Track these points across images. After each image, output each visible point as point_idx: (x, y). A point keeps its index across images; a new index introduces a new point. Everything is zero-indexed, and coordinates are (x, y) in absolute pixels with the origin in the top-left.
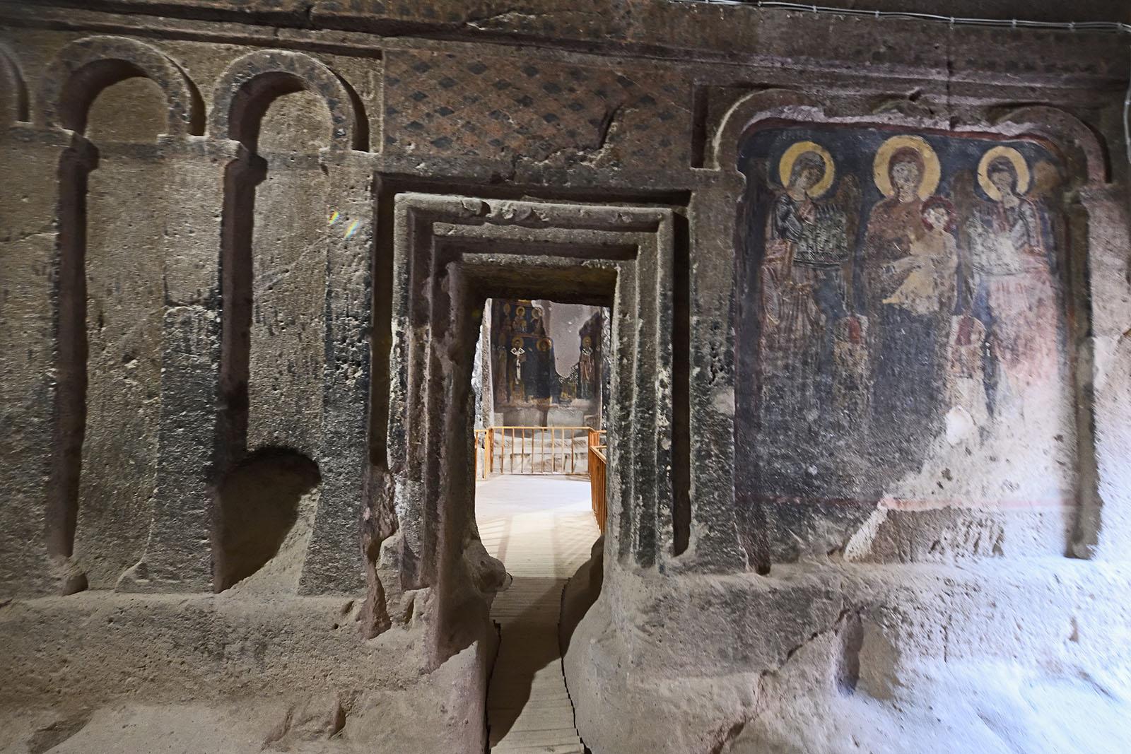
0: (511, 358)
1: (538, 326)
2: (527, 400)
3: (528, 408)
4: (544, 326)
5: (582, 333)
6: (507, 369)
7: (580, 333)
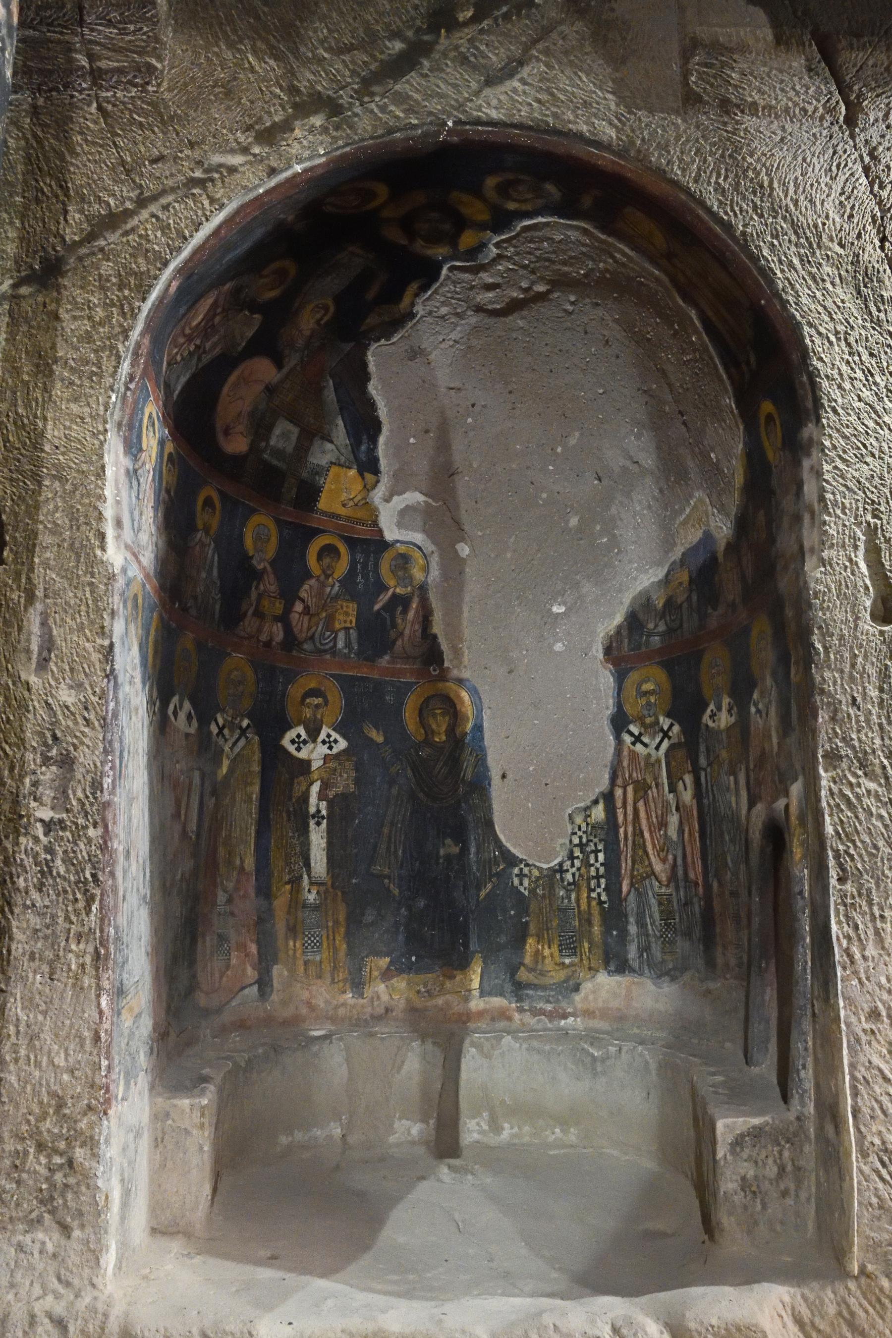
0: (281, 774)
1: (408, 623)
2: (358, 984)
3: (364, 1024)
4: (437, 628)
6: (264, 825)
7: (608, 651)
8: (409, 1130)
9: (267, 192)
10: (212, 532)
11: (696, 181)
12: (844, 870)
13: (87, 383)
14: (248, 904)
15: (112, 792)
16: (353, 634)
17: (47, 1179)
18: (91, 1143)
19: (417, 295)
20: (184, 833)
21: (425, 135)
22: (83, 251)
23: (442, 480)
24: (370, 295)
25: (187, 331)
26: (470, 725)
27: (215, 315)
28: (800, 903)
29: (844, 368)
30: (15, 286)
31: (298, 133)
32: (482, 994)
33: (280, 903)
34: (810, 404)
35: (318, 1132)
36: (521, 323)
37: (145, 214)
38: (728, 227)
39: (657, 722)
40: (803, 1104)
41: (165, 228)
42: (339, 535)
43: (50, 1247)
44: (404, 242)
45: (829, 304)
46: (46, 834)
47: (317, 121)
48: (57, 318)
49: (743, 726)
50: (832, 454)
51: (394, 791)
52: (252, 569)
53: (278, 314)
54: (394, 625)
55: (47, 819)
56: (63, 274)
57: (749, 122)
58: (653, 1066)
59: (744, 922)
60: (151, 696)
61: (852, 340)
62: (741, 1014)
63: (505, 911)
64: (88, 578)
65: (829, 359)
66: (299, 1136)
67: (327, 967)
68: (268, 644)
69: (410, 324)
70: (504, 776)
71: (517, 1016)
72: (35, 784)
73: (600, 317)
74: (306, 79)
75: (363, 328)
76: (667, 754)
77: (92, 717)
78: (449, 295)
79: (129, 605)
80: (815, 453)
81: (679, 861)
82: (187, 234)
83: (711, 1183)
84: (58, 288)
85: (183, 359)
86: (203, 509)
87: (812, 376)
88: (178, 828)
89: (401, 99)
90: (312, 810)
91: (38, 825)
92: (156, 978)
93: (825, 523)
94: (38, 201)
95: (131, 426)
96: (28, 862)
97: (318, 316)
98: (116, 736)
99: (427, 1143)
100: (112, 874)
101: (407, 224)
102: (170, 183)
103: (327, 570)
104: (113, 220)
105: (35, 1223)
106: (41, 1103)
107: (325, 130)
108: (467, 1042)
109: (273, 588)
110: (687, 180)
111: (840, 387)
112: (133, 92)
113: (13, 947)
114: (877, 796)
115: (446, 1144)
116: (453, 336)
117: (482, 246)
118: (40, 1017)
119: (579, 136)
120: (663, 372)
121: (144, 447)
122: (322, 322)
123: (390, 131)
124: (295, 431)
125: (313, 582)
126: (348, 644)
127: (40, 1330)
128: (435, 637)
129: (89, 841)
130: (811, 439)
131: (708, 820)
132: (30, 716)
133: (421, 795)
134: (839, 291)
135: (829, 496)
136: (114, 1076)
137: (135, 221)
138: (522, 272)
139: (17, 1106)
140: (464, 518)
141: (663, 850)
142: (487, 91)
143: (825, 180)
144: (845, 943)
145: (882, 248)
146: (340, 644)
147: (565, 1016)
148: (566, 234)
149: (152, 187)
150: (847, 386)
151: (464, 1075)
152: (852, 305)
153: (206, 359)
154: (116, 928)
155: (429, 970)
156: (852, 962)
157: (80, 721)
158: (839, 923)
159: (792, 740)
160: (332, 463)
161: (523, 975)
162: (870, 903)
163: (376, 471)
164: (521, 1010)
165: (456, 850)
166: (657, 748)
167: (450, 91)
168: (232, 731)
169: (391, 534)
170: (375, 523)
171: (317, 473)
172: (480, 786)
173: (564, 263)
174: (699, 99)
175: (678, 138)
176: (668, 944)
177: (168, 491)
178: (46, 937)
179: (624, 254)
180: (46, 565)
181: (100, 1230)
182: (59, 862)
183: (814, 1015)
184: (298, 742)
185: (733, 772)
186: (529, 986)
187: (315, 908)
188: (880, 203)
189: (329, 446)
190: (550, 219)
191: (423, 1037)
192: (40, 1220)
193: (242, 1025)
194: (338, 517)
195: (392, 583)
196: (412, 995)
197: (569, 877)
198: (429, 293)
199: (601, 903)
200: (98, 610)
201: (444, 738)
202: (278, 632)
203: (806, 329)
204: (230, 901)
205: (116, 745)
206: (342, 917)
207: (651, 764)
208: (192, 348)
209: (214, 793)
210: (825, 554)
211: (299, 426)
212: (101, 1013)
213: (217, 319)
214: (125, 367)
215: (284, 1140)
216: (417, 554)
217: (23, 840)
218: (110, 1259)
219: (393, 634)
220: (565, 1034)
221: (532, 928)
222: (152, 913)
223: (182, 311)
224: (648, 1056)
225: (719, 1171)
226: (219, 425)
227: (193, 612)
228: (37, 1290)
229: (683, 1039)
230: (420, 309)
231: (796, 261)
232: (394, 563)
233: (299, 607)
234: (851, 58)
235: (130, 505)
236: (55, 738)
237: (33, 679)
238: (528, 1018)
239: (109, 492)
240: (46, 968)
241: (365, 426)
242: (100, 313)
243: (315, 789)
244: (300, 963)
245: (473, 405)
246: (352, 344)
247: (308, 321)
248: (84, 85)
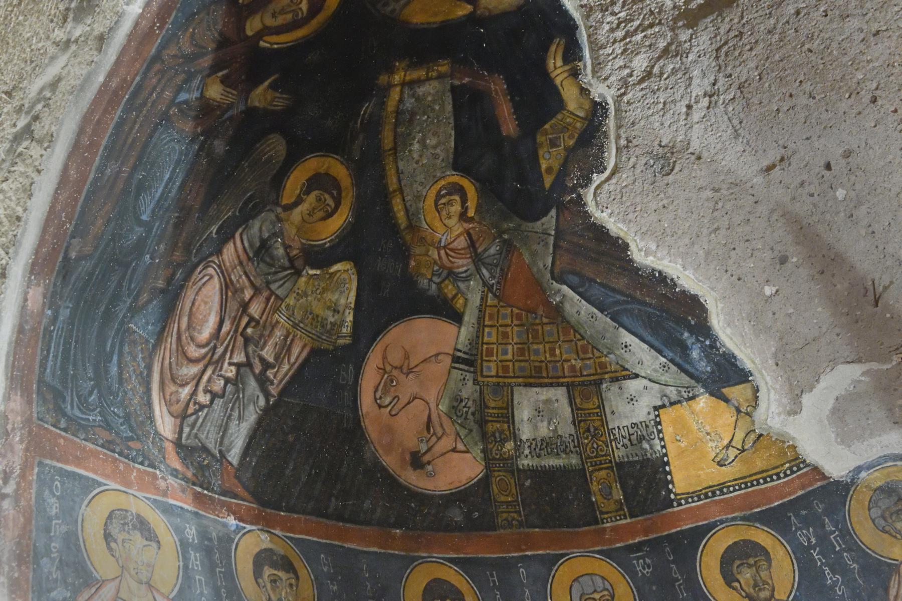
9: (110, 75)
19: (575, 74)
24: (509, 126)
27: (245, 306)
42: (743, 518)
69: (611, 122)
75: (548, 181)
78: (620, 34)
82: (19, 210)
85: (214, 396)
97: (456, 208)
122: (471, 213)
124: (559, 395)
160: (656, 408)
163: (743, 376)
169: (837, 465)
170: (798, 461)
171: (641, 439)
189: (633, 386)
194: (722, 487)
198: (587, 53)
211: (559, 385)
213: (255, 309)
223: (142, 328)
226: (390, 461)
230: (600, 91)
232: (876, 512)
241: (673, 318)
245: (828, 167)
246: (553, 212)
247: (445, 223)
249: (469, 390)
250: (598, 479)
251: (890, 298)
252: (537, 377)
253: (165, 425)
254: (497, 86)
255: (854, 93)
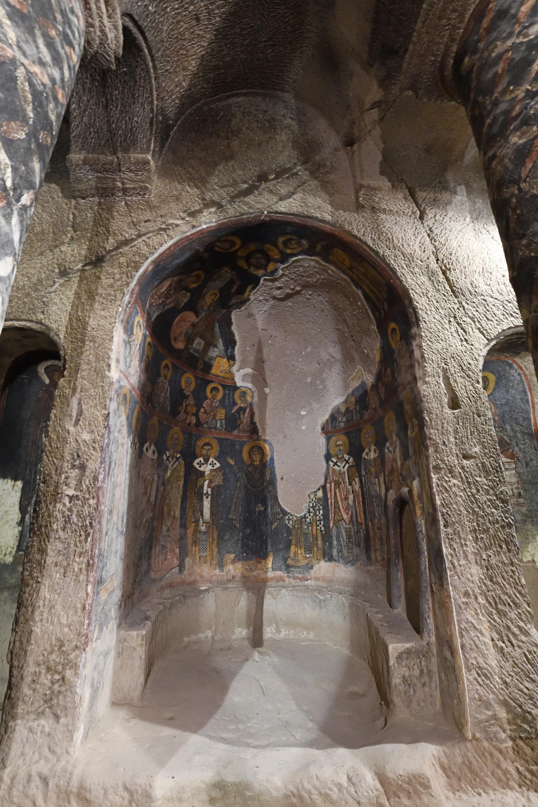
0: (192, 476)
1: (245, 418)
2: (221, 565)
3: (223, 584)
4: (257, 420)
5: (328, 430)
6: (184, 498)
8: (242, 633)
10: (168, 377)
11: (363, 236)
12: (446, 522)
13: (109, 303)
14: (176, 532)
15: (103, 482)
16: (224, 421)
17: (50, 688)
18: (75, 667)
19: (251, 291)
20: (149, 501)
21: (255, 217)
22: (113, 253)
23: (259, 364)
24: (233, 290)
25: (158, 294)
26: (269, 458)
27: (170, 290)
28: (421, 537)
29: (427, 306)
30: (83, 266)
31: (205, 214)
32: (273, 569)
33: (190, 531)
34: (414, 320)
35: (201, 635)
36: (290, 304)
37: (140, 240)
38: (377, 253)
39: (343, 457)
40: (430, 637)
41: (148, 245)
43: (47, 729)
44: (246, 267)
45: (419, 282)
46: (70, 502)
47: (213, 210)
48: (100, 278)
49: (382, 457)
50: (426, 339)
51: (238, 485)
52: (184, 394)
53: (197, 295)
54: (240, 418)
55: (71, 495)
56: (104, 262)
57: (383, 216)
58: (347, 605)
59: (385, 541)
60: (134, 440)
61: (429, 296)
62: (385, 582)
63: (282, 534)
64: (101, 384)
65: (421, 302)
66: (193, 637)
67: (208, 558)
68: (189, 424)
69: (248, 303)
70: (282, 479)
71: (287, 580)
72: (67, 478)
73: (320, 300)
74: (209, 196)
76: (348, 470)
77: (96, 446)
79: (121, 397)
80: (417, 339)
81: (354, 514)
83: (386, 676)
84: (101, 267)
86: (164, 368)
87: (414, 309)
88: (145, 499)
89: (246, 204)
90: (205, 492)
91: (67, 498)
92: (127, 569)
93: (425, 367)
94: (97, 235)
95: (128, 322)
96: (59, 516)
97: (213, 297)
98: (107, 456)
99: (249, 639)
100: (100, 522)
101: (247, 259)
102: (152, 229)
103: (214, 397)
104: (126, 242)
105: (40, 714)
106: (51, 644)
107: (216, 213)
108: (266, 592)
109: (192, 402)
110: (360, 235)
111: (426, 313)
112: (140, 197)
113: (47, 559)
114: (459, 487)
115: (257, 640)
116: (264, 309)
117: (276, 270)
118: (56, 596)
119: (317, 219)
120: (345, 320)
121: (135, 332)
123: (242, 214)
124: (203, 342)
125: (208, 401)
126: (221, 426)
127: (32, 785)
128: (255, 423)
129: (90, 506)
130: (415, 334)
131: (366, 497)
132: (68, 445)
133: (249, 486)
134: (422, 278)
135: (426, 355)
136: (91, 628)
137: (136, 243)
138: (292, 281)
139: (38, 647)
140: (267, 378)
141: (347, 509)
142: (280, 202)
143: (413, 238)
144: (450, 557)
145: (437, 263)
146: (218, 425)
147: (307, 580)
148: (308, 263)
149: (144, 230)
150: (429, 312)
151: (265, 607)
152: (428, 283)
153: (167, 307)
154: (100, 550)
155: (251, 559)
156: (454, 567)
157: (91, 448)
158: (446, 547)
159: (410, 463)
161: (290, 562)
162: (460, 538)
164: (289, 577)
165: (262, 509)
166: (344, 467)
167: (266, 202)
168: (172, 458)
169: (239, 383)
172: (272, 482)
173: (308, 277)
174: (363, 207)
175: (355, 220)
176: (349, 549)
177: (148, 357)
178: (64, 555)
179: (332, 271)
180: (83, 378)
181: (75, 718)
182: (74, 516)
183: (432, 591)
184: (200, 464)
185: (377, 477)
186: (292, 566)
187: (205, 533)
188: (435, 247)
189: (216, 349)
190: (303, 257)
191: (248, 589)
192: (43, 713)
193: (171, 585)
194: (219, 376)
195: (239, 402)
196: (244, 571)
197: (308, 520)
199: (321, 531)
200: (104, 398)
201: (258, 463)
202: (194, 420)
203: (411, 291)
204: (168, 530)
205: (107, 460)
206: (216, 536)
207: (341, 474)
208: (161, 302)
209: (163, 484)
210: (427, 379)
212: (87, 594)
213: (171, 292)
214: (127, 298)
215: (186, 639)
216: (249, 391)
217: (58, 505)
218: (79, 736)
219: (239, 422)
220: (307, 588)
221: (293, 542)
222: (126, 539)
223: (156, 283)
224: (344, 600)
225: (391, 673)
227: (158, 409)
228: (36, 757)
229: (358, 592)
230: (252, 297)
231: (404, 266)
233: (202, 410)
234: (421, 195)
235: (125, 355)
236: (78, 456)
237: (72, 429)
238: (291, 580)
239: (114, 347)
240: (62, 570)
241: (230, 342)
242: (118, 276)
243: (206, 483)
244: (197, 557)
247: (209, 299)
248: (120, 194)
249: (190, 331)
250: (200, 362)
251: (265, 363)
252: (203, 337)
253: (148, 306)
254: (238, 283)
255: (284, 328)
